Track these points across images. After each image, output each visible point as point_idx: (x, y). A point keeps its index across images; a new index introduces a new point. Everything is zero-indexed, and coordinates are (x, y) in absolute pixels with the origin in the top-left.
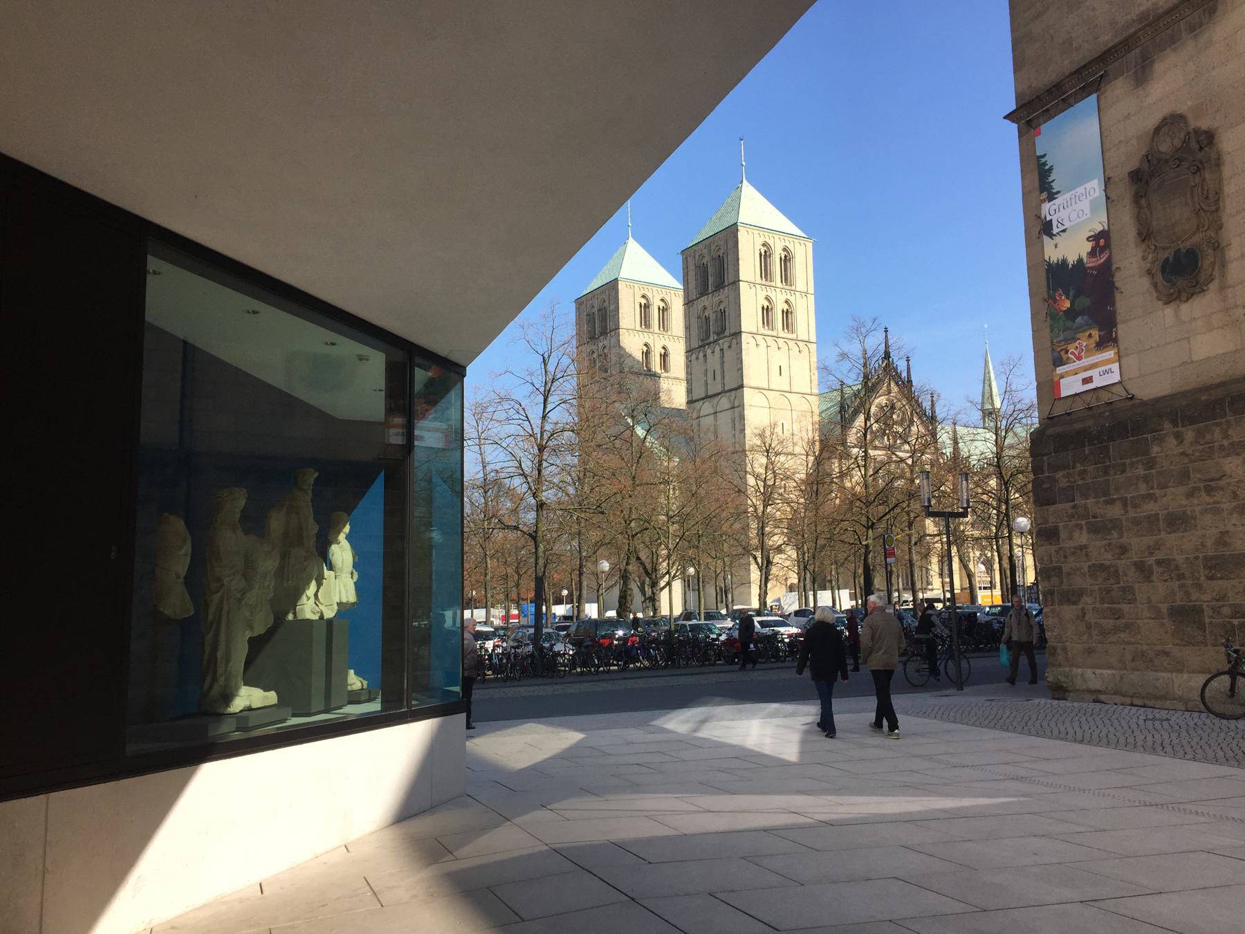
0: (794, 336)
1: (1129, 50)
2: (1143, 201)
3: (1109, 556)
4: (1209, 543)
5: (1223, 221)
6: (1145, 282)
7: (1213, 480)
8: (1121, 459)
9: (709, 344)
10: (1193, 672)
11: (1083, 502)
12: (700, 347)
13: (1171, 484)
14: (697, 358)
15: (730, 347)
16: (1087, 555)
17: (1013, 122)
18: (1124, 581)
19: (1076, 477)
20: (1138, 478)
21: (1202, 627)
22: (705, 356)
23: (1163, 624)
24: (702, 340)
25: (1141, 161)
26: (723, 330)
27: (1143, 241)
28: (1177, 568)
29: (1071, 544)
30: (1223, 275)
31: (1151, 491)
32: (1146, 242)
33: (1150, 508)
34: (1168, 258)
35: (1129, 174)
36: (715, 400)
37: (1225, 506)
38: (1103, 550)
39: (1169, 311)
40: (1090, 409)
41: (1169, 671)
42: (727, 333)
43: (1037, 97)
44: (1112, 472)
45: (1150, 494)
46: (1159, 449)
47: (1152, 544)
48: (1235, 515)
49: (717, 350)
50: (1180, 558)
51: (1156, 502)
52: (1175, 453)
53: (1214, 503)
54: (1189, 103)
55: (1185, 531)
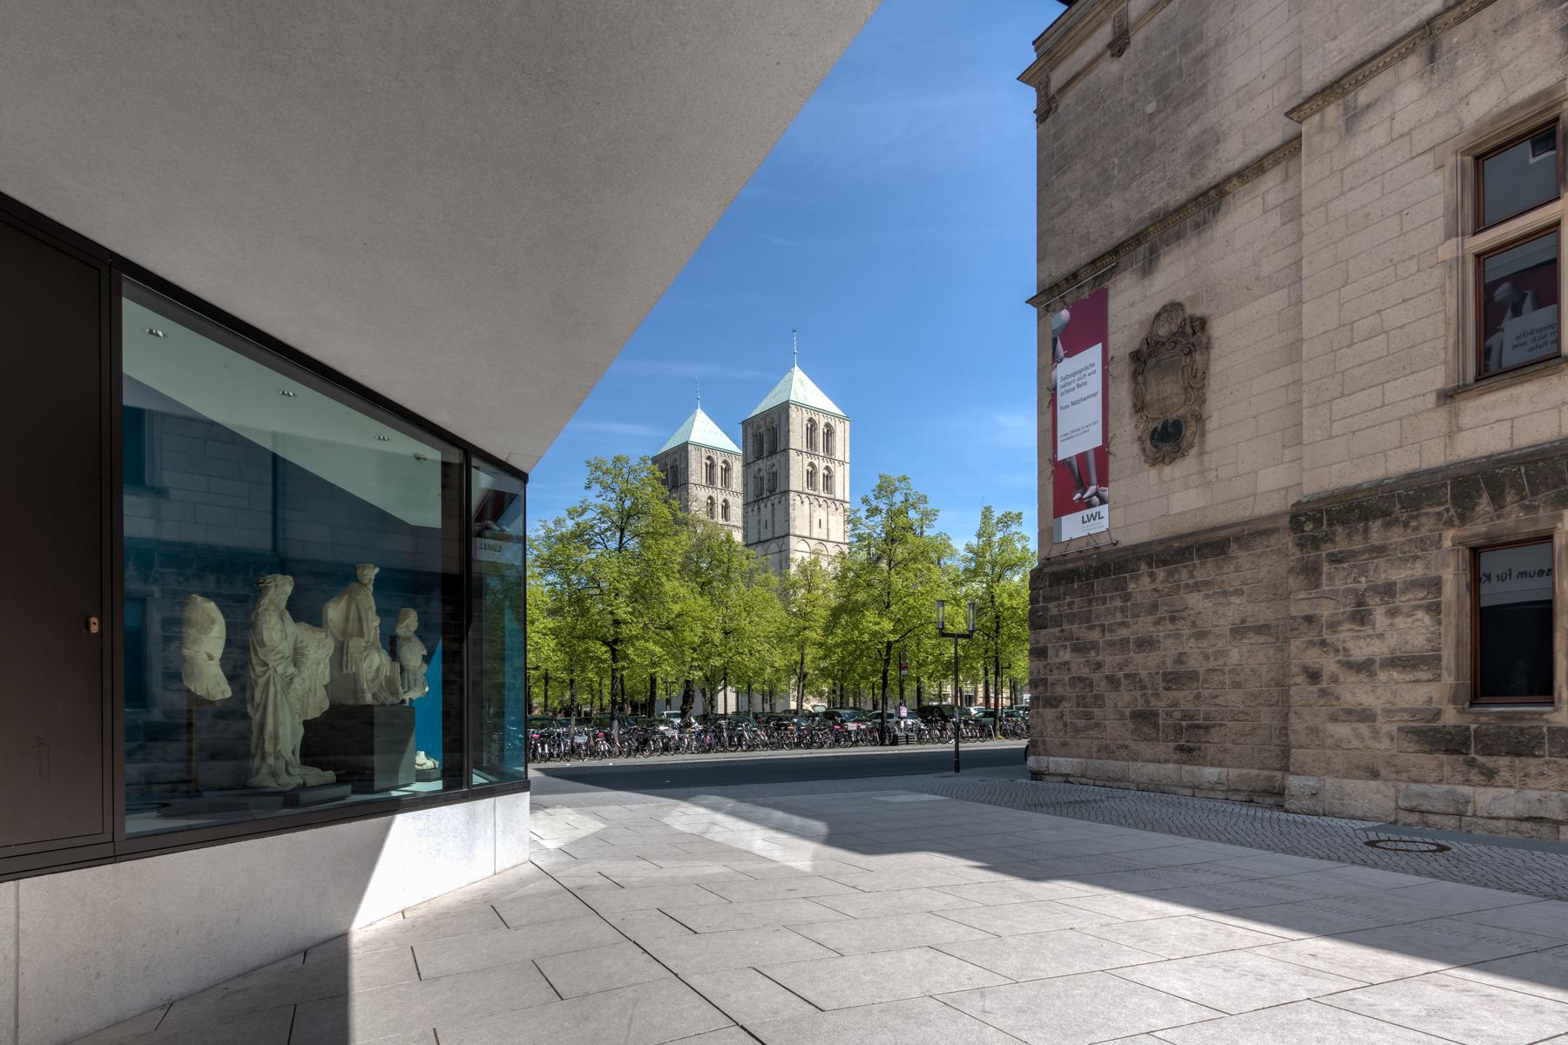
0: (832, 496)
1: (1140, 244)
2: (1140, 378)
3: (1086, 670)
4: (1169, 661)
5: (1207, 397)
7: (1176, 611)
9: (763, 499)
10: (1146, 761)
12: (755, 501)
13: (1142, 614)
14: (753, 511)
15: (780, 502)
16: (1069, 670)
17: (1034, 306)
18: (1097, 691)
19: (1066, 607)
20: (1116, 608)
21: (1156, 726)
22: (759, 509)
23: (1125, 724)
24: (757, 496)
25: (1142, 343)
26: (774, 490)
27: (1137, 412)
28: (1141, 680)
29: (1057, 660)
30: (1202, 443)
33: (1124, 633)
34: (1157, 427)
36: (767, 544)
37: (1184, 632)
38: (1082, 666)
39: (1153, 472)
41: (1127, 761)
42: (778, 491)
43: (1056, 284)
44: (1095, 604)
46: (1135, 586)
48: (1192, 640)
49: (769, 504)
50: (1143, 673)
51: (1128, 628)
53: (1176, 630)
54: (1188, 293)
55: (1150, 651)
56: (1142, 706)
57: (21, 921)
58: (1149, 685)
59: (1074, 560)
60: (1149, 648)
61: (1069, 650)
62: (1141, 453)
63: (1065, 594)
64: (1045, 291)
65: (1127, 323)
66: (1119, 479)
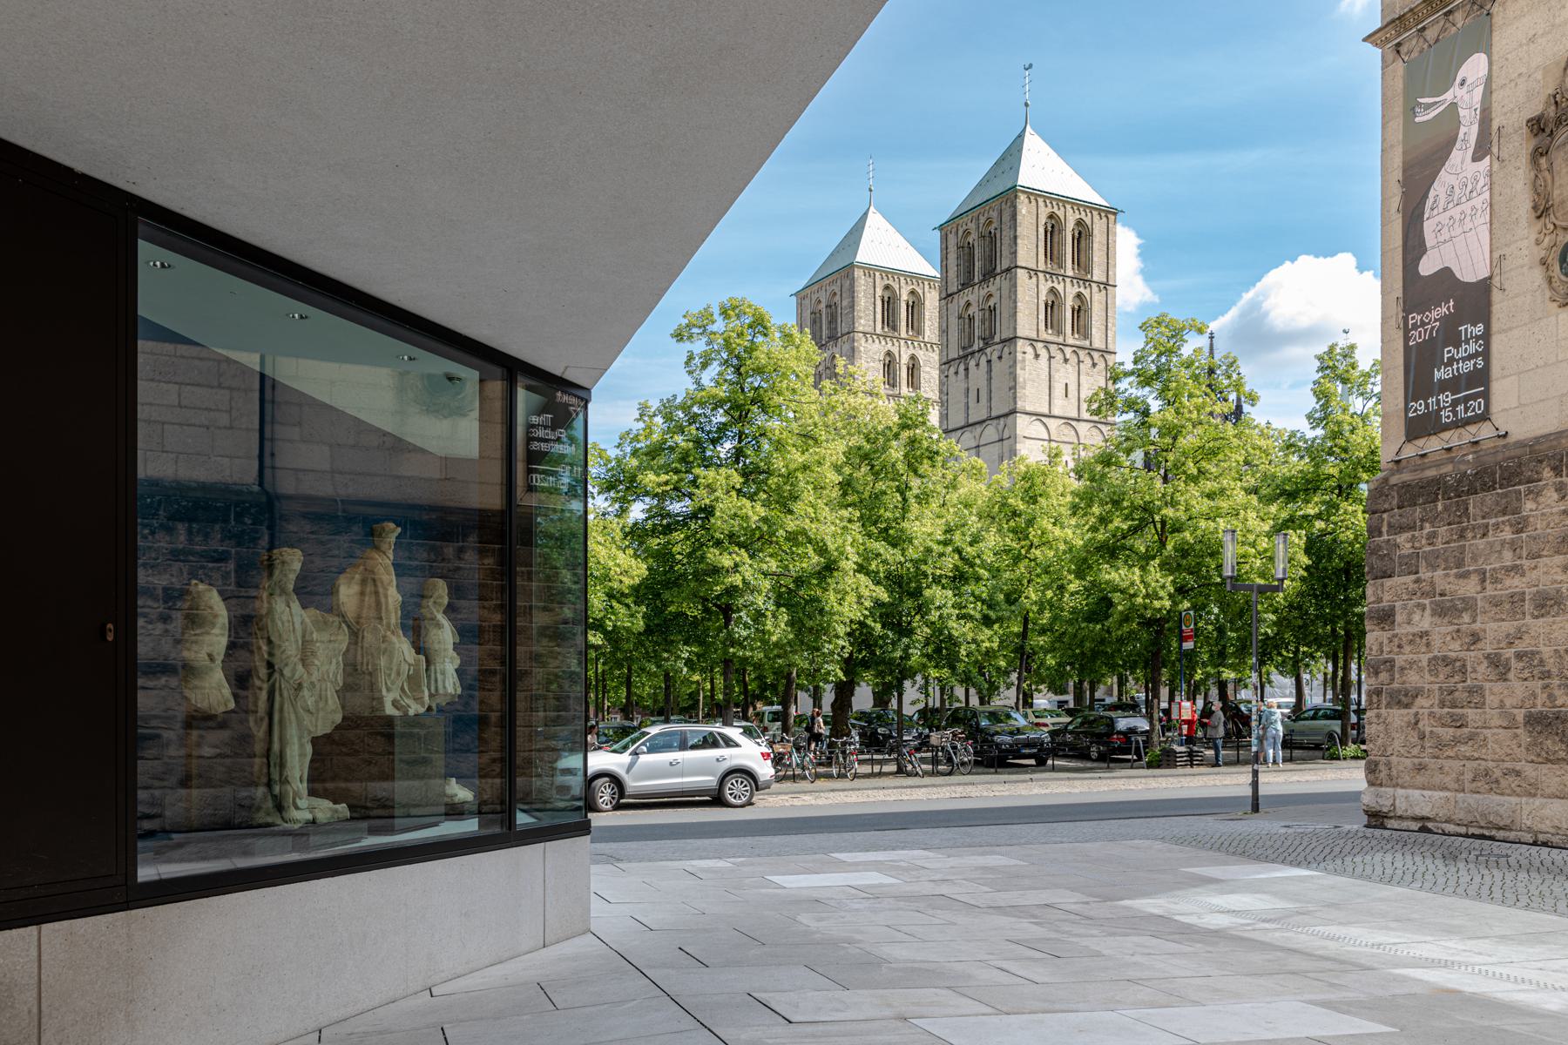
2: (1543, 161)
3: (1456, 646)
6: (1538, 275)
8: (1484, 518)
9: (973, 353)
11: (1430, 574)
12: (960, 358)
13: (1545, 553)
14: (956, 373)
15: (1000, 358)
16: (1428, 645)
18: (1472, 679)
19: (1424, 541)
20: (1503, 543)
22: (967, 369)
23: (1516, 736)
24: (964, 348)
27: (1539, 217)
28: (1541, 661)
29: (1410, 629)
31: (1518, 562)
32: (1543, 219)
33: (1515, 583)
35: (1528, 122)
40: (1449, 450)
41: (1518, 795)
42: (997, 339)
43: (1411, 10)
44: (1470, 535)
45: (1517, 566)
46: (1534, 506)
47: (1512, 631)
49: (983, 360)
50: (1546, 651)
51: (1523, 575)
52: (1555, 510)
55: (1558, 614)
56: (1543, 705)
58: (1555, 671)
59: (1438, 465)
60: (1556, 608)
61: (1428, 612)
62: (1545, 285)
63: (1422, 520)
64: (1393, 21)
65: (1524, 70)
66: (1510, 329)
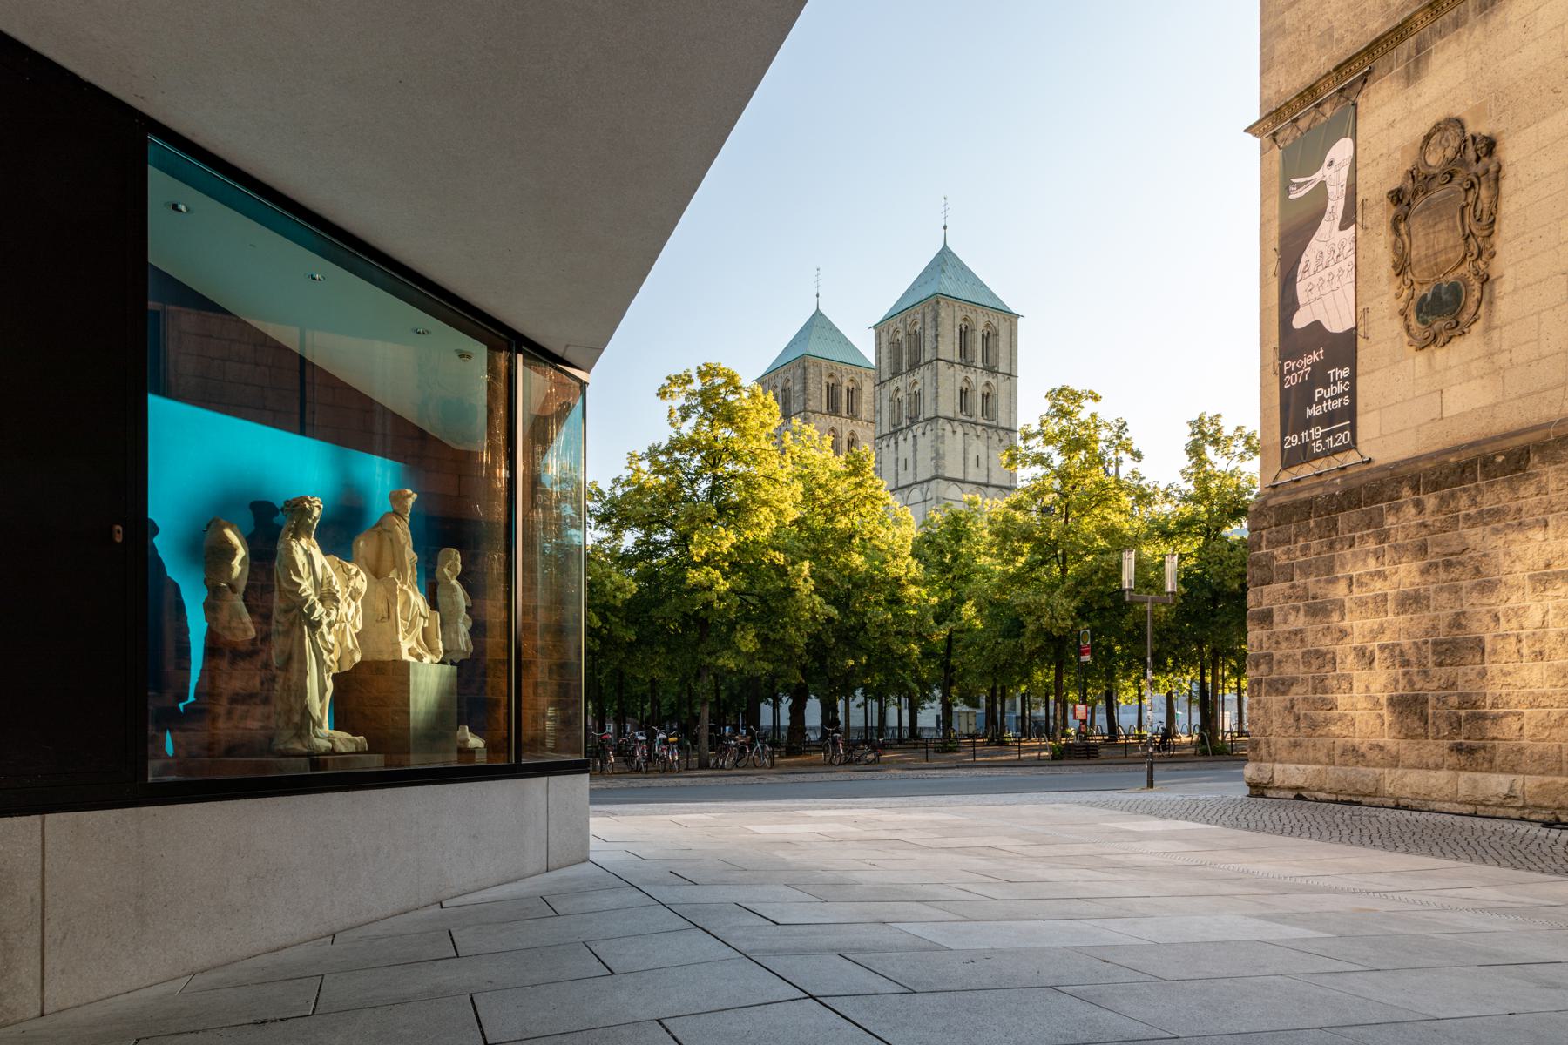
1: (1402, 39)
4: (1443, 626)
5: (1496, 248)
6: (1398, 324)
7: (1452, 554)
8: (1350, 532)
10: (1408, 767)
11: (1303, 581)
12: (891, 433)
14: (888, 446)
15: (924, 434)
16: (1302, 640)
19: (1298, 553)
20: (1368, 552)
21: (1424, 718)
22: (896, 443)
25: (1406, 177)
26: (917, 417)
27: (1398, 275)
28: (1402, 653)
29: (1286, 628)
30: (1490, 314)
31: (1381, 568)
32: (1401, 277)
33: (1379, 586)
34: (1426, 295)
35: (1389, 193)
37: (1464, 583)
38: (1320, 634)
39: (1421, 358)
40: (1319, 475)
41: (1382, 767)
42: (921, 418)
43: (1286, 104)
44: (1338, 546)
45: (1379, 571)
46: (1395, 520)
47: (1376, 627)
48: (1475, 594)
52: (1412, 523)
53: (1452, 580)
54: (1470, 103)
56: (1403, 690)
57: (47, 860)
58: (1413, 659)
59: (1310, 488)
60: (1414, 606)
61: (1302, 612)
62: (1404, 333)
63: (1297, 536)
64: (1270, 114)
65: (1384, 151)
66: (1373, 371)
